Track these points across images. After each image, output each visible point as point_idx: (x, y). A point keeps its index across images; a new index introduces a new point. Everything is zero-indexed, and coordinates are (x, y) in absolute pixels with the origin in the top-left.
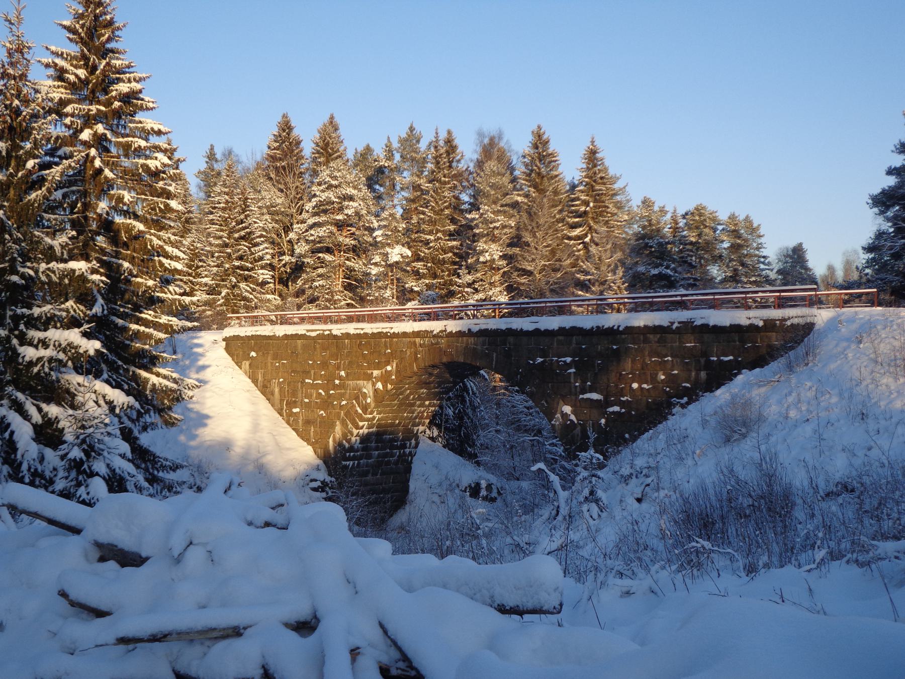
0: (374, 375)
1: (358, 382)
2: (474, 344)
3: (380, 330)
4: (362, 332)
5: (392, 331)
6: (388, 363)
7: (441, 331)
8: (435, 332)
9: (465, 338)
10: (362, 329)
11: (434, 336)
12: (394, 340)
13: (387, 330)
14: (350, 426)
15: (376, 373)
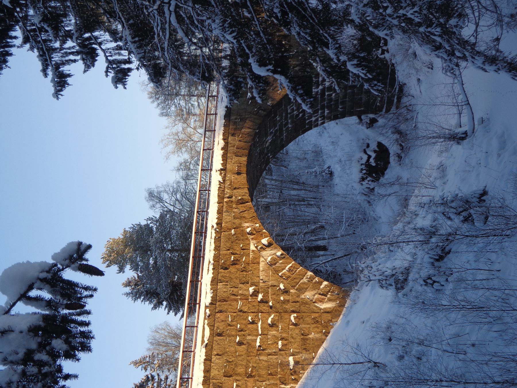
0: (255, 249)
1: (261, 269)
2: (234, 146)
3: (213, 241)
4: (212, 262)
5: (215, 226)
6: (243, 233)
7: (221, 174)
8: (221, 180)
9: (228, 155)
10: (210, 262)
11: (224, 180)
12: (223, 225)
13: (214, 232)
14: (305, 280)
15: (252, 247)
